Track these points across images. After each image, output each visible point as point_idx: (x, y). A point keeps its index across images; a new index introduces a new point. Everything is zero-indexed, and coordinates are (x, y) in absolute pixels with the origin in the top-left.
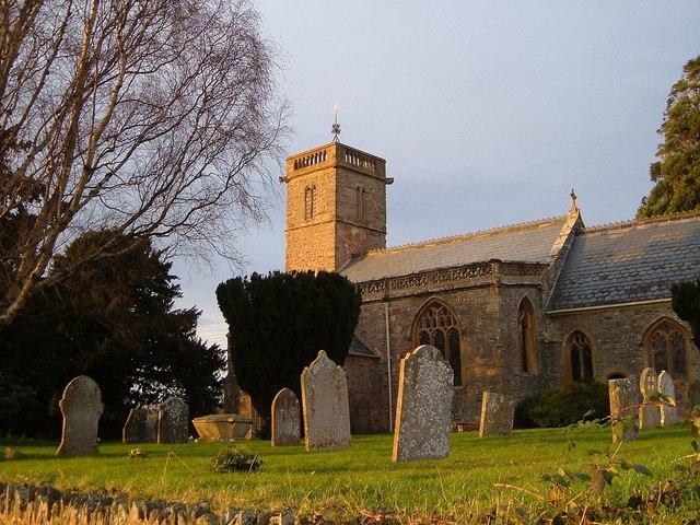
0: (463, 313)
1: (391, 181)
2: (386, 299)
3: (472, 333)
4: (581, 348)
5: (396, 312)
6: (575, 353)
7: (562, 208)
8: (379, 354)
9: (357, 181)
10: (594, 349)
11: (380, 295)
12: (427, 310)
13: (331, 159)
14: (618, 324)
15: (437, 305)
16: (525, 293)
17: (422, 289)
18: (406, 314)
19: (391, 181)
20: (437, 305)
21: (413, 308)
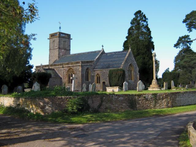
0: (75, 70)
1: (72, 39)
2: (63, 67)
3: (77, 74)
4: (99, 77)
5: (65, 69)
6: (98, 78)
7: (100, 49)
8: (62, 77)
9: (64, 40)
10: (100, 77)
11: (62, 66)
12: (69, 69)
13: (58, 36)
14: (104, 73)
15: (71, 69)
16: (88, 67)
17: (69, 66)
18: (66, 70)
19: (72, 39)
20: (71, 69)
21: (67, 69)
